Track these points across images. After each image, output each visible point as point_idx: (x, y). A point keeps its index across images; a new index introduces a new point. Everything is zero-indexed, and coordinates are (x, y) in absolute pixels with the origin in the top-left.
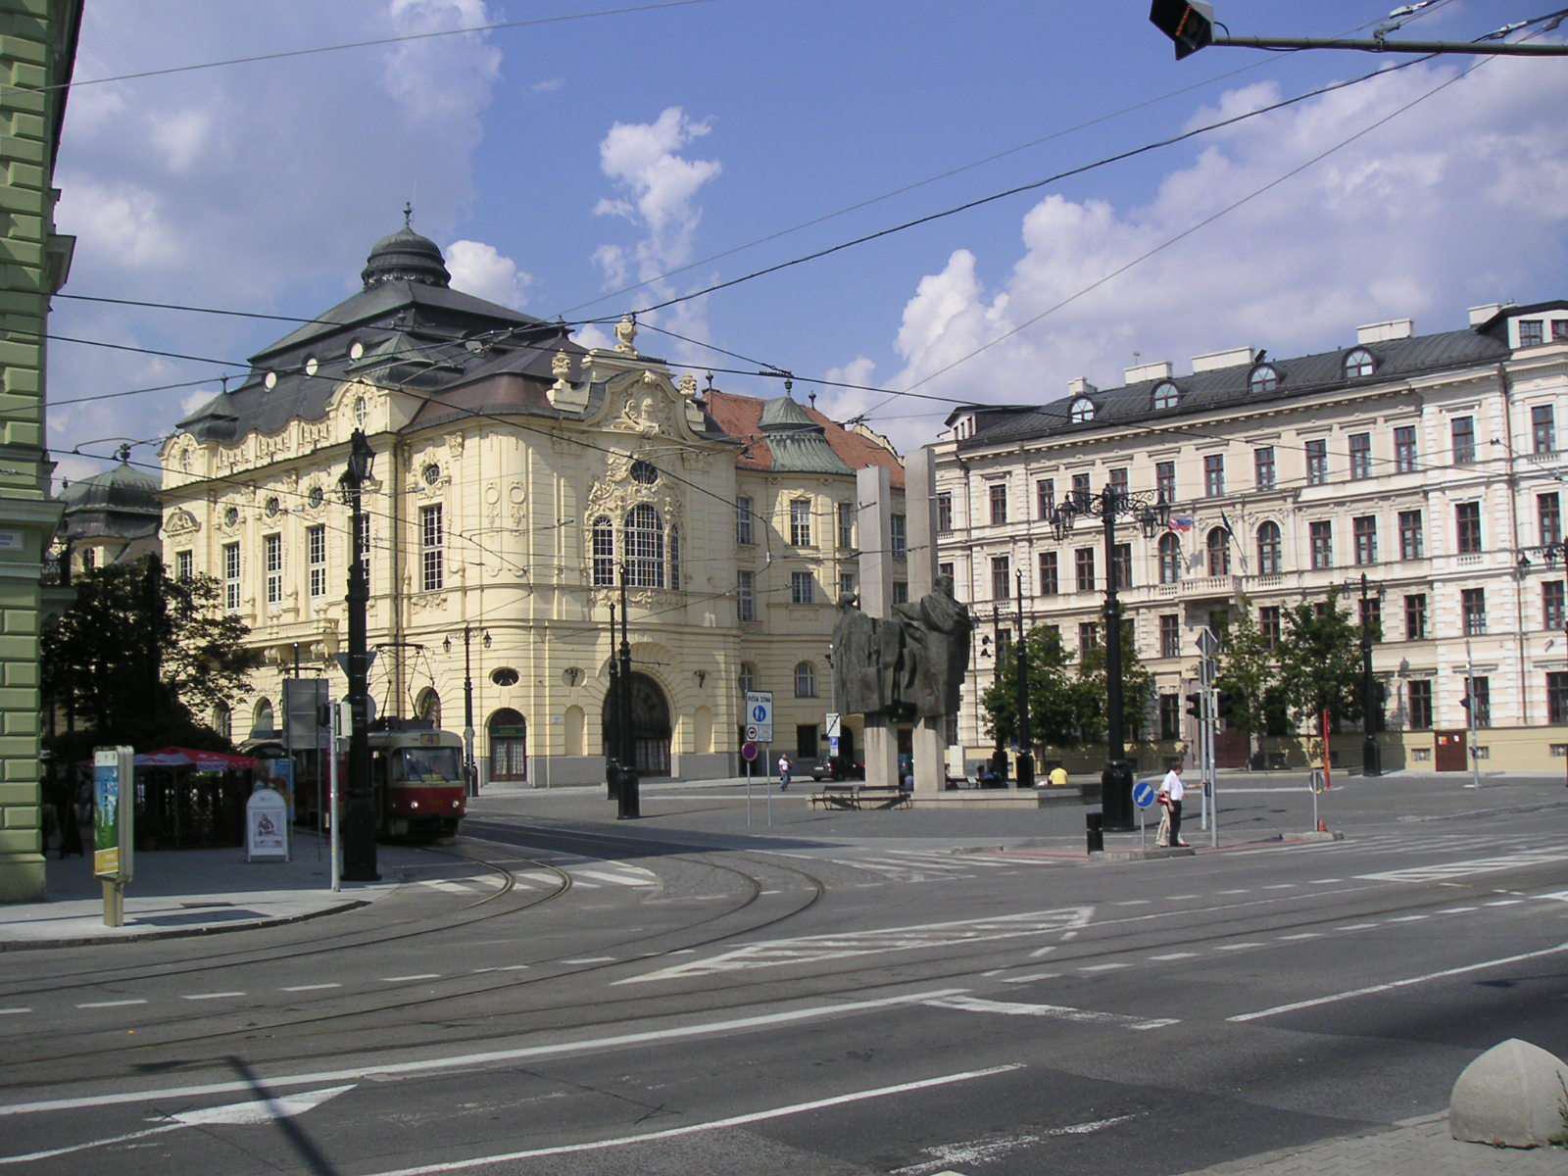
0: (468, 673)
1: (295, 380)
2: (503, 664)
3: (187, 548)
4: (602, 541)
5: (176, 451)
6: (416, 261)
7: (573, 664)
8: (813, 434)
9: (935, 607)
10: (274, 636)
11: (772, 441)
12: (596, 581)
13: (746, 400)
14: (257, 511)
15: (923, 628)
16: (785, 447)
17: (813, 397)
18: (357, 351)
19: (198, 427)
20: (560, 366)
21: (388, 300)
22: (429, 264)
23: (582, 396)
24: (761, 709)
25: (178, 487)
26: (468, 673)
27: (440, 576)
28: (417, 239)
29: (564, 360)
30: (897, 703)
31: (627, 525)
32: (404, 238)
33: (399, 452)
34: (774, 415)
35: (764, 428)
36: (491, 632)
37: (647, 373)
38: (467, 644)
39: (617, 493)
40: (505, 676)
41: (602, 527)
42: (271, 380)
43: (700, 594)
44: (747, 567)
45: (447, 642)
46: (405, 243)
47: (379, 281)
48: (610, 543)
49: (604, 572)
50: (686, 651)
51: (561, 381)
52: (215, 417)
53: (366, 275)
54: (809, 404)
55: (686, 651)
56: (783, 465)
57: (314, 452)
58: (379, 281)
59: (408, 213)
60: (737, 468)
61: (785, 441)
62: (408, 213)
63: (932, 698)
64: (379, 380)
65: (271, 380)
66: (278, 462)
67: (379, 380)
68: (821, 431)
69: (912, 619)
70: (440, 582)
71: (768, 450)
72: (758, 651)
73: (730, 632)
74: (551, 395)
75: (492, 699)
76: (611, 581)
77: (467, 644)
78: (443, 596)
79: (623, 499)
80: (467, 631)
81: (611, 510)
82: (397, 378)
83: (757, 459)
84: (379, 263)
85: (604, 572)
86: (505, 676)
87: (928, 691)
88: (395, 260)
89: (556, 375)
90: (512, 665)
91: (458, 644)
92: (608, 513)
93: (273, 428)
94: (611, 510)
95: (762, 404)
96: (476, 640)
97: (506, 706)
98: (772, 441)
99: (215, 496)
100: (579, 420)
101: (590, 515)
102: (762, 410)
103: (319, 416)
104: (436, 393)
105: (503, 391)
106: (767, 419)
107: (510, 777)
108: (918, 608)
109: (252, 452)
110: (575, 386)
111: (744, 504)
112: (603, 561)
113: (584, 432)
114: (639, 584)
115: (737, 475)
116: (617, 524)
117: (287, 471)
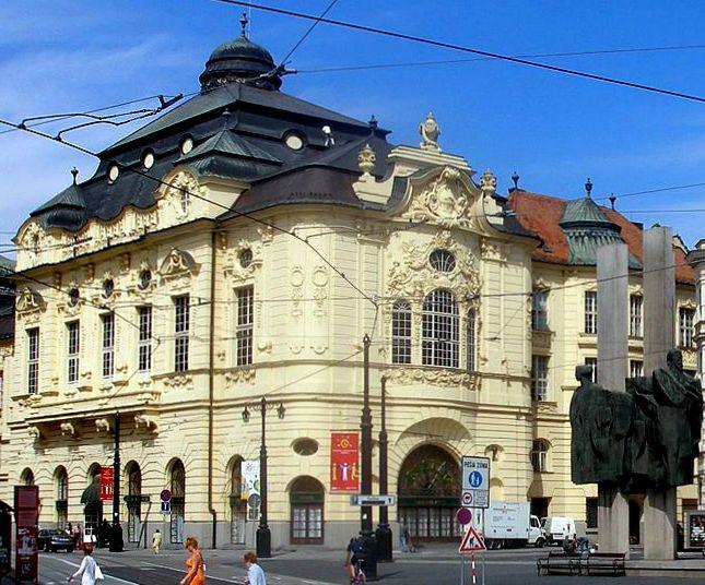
0: (263, 442)
1: (131, 176)
2: (304, 434)
3: (35, 325)
4: (401, 324)
5: (28, 237)
8: (610, 232)
9: (666, 381)
10: (105, 407)
11: (571, 237)
12: (395, 360)
13: (549, 200)
14: (95, 292)
15: (654, 401)
16: (583, 242)
17: (613, 200)
18: (188, 146)
19: (47, 215)
20: (367, 160)
21: (220, 100)
23: (387, 187)
24: (477, 475)
25: (28, 270)
26: (263, 442)
27: (250, 353)
28: (250, 46)
29: (369, 154)
30: (627, 473)
31: (425, 309)
32: (239, 45)
33: (217, 237)
34: (575, 213)
35: (565, 226)
36: (285, 406)
37: (447, 169)
38: (263, 415)
40: (305, 446)
42: (114, 173)
43: (492, 376)
44: (541, 351)
45: (246, 413)
46: (241, 50)
47: (215, 84)
48: (409, 325)
49: (402, 352)
50: (478, 427)
51: (366, 174)
52: (60, 206)
53: (203, 78)
54: (608, 205)
55: (478, 427)
56: (580, 260)
57: (142, 237)
58: (215, 84)
59: (244, 23)
60: (533, 260)
61: (583, 238)
62: (244, 23)
63: (660, 471)
64: (201, 171)
65: (114, 173)
66: (114, 246)
67: (201, 171)
68: (617, 229)
69: (646, 392)
70: (250, 358)
71: (566, 245)
72: (552, 430)
73: (522, 411)
74: (356, 186)
75: (288, 467)
76: (408, 360)
77: (263, 415)
78: (252, 371)
80: (264, 403)
82: (218, 169)
83: (556, 253)
85: (402, 352)
86: (305, 446)
87: (658, 463)
89: (362, 168)
90: (312, 436)
91: (255, 414)
93: (111, 219)
95: (564, 205)
96: (272, 412)
98: (571, 237)
99: (60, 278)
100: (381, 210)
102: (565, 210)
103: (149, 206)
104: (253, 184)
105: (318, 181)
106: (568, 218)
107: (308, 540)
108: (650, 381)
109: (96, 236)
110: (379, 178)
111: (538, 294)
113: (388, 221)
114: (435, 363)
115: (533, 267)
116: (416, 308)
117: (121, 255)
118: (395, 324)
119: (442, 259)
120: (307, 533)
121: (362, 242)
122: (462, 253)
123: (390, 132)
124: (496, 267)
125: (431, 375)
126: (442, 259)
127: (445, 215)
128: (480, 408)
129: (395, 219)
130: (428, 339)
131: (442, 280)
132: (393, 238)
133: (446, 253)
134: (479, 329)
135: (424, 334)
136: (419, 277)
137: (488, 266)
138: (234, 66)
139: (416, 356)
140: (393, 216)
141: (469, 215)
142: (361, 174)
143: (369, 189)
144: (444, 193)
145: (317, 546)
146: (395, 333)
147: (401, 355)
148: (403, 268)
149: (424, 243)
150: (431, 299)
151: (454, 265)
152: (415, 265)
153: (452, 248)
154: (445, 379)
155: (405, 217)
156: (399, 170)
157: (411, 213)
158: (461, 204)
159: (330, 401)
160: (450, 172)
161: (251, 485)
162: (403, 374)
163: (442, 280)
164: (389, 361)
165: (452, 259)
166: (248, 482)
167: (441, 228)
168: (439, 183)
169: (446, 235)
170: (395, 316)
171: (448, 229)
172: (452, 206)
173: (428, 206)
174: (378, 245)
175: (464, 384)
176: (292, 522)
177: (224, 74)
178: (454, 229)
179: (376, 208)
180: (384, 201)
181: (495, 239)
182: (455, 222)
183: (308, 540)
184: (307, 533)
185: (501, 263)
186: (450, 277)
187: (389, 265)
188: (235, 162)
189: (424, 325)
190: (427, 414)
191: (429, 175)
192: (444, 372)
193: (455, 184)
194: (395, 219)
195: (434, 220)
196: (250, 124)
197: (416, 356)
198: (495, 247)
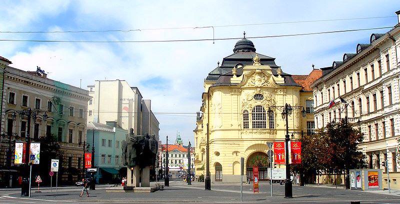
4: (246, 117)
6: (246, 46)
7: (218, 151)
22: (249, 47)
40: (218, 154)
48: (248, 117)
74: (232, 79)
84: (237, 47)
88: (242, 46)
92: (247, 109)
107: (219, 180)
116: (250, 112)
118: (244, 117)
119: (258, 96)
121: (232, 95)
125: (254, 131)
127: (258, 84)
131: (259, 103)
132: (242, 93)
134: (276, 117)
135: (253, 119)
136: (251, 102)
142: (233, 75)
143: (235, 80)
144: (257, 77)
147: (246, 126)
149: (252, 93)
155: (245, 86)
157: (247, 84)
160: (257, 71)
163: (259, 103)
164: (242, 128)
167: (257, 87)
169: (259, 89)
170: (244, 115)
177: (239, 49)
178: (261, 87)
179: (236, 85)
180: (240, 82)
183: (219, 180)
189: (253, 117)
191: (253, 72)
193: (260, 74)
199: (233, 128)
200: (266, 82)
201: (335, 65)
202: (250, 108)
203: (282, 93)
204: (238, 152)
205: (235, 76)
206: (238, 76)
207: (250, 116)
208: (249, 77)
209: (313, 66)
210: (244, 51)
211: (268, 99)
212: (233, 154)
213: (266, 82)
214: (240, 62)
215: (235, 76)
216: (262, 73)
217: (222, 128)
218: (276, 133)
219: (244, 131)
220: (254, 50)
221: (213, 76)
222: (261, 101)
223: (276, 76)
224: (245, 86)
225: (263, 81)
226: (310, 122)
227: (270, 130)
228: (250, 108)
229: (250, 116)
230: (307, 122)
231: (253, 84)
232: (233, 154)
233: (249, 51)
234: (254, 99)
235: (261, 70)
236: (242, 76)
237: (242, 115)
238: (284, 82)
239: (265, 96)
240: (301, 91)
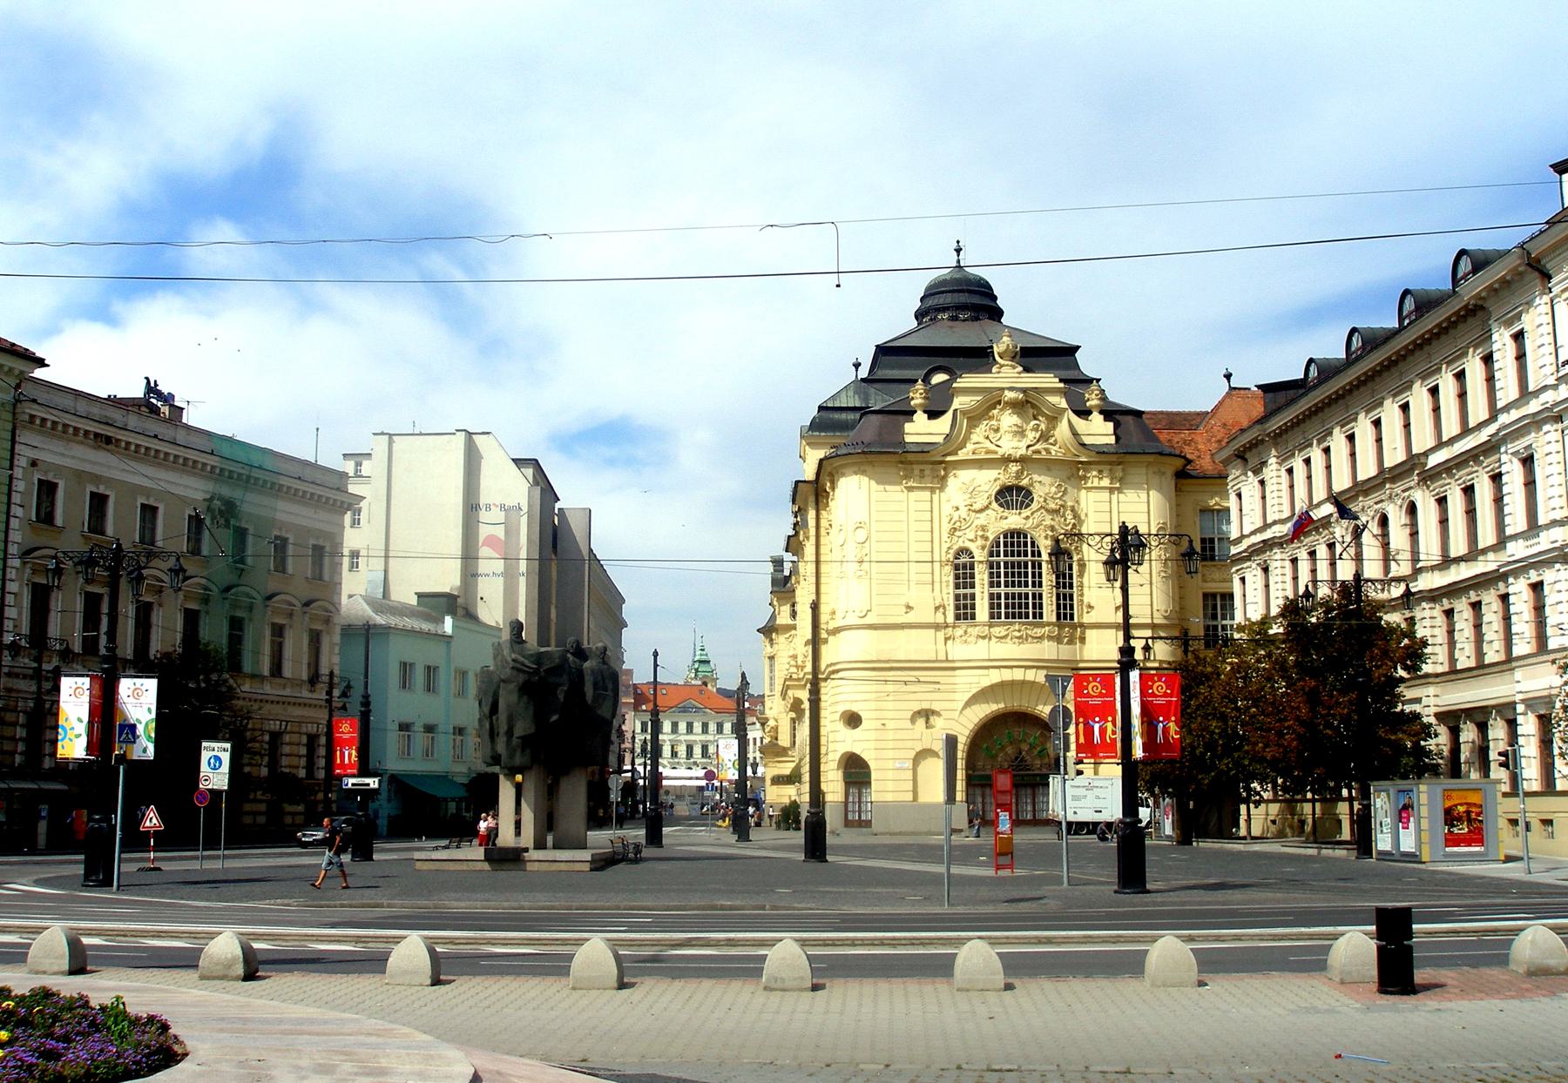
4: (963, 574)
6: (963, 298)
7: (855, 708)
12: (957, 617)
22: (976, 300)
37: (1006, 392)
39: (977, 522)
40: (853, 720)
41: (964, 559)
48: (972, 576)
49: (965, 607)
74: (908, 427)
79: (983, 528)
81: (971, 540)
84: (930, 302)
85: (965, 607)
92: (969, 545)
94: (971, 540)
97: (858, 752)
101: (949, 548)
112: (965, 596)
115: (1178, 490)
116: (980, 555)
118: (957, 577)
119: (1013, 496)
120: (860, 816)
121: (910, 489)
122: (1043, 486)
123: (1078, 347)
124: (1105, 495)
125: (998, 631)
126: (1013, 496)
127: (1011, 445)
128: (1081, 665)
129: (949, 458)
130: (995, 590)
131: (1014, 520)
132: (951, 481)
133: (1020, 489)
134: (1081, 575)
135: (991, 585)
136: (982, 519)
137: (1093, 495)
138: (936, 301)
139: (982, 611)
140: (945, 455)
141: (1051, 441)
142: (915, 412)
143: (920, 429)
144: (1008, 420)
145: (864, 830)
146: (957, 586)
147: (965, 611)
148: (963, 512)
149: (989, 480)
150: (998, 546)
151: (1032, 500)
152: (977, 507)
153: (1024, 482)
154: (1017, 634)
155: (962, 455)
156: (959, 402)
157: (970, 447)
158: (1036, 429)
159: (874, 669)
160: (1009, 395)
161: (730, 764)
162: (966, 632)
163: (1014, 520)
164: (951, 618)
165: (1029, 493)
166: (726, 761)
167: (1006, 460)
168: (1001, 410)
169: (1014, 468)
170: (957, 567)
171: (1016, 461)
172: (1021, 433)
173: (987, 438)
174: (932, 490)
175: (1050, 638)
176: (846, 803)
178: (1022, 460)
179: (924, 449)
181: (1099, 463)
182: (1023, 451)
184: (860, 816)
185: (1111, 490)
186: (1024, 515)
187: (947, 510)
188: (844, 416)
189: (991, 575)
190: (995, 677)
191: (992, 401)
192: (1017, 627)
193: (1017, 407)
194: (949, 458)
195: (996, 453)
196: (893, 368)
197: (982, 611)
198: (1100, 472)
199: (911, 618)
200: (1044, 437)
201: (1313, 372)
202: (980, 542)
203: (1106, 482)
204: (934, 712)
205: (920, 417)
206: (933, 414)
207: (981, 576)
208: (975, 417)
209: (1228, 376)
210: (954, 319)
211: (1052, 506)
212: (913, 720)
213: (1044, 437)
214: (940, 361)
215: (920, 417)
216: (1027, 404)
217: (869, 620)
218: (1083, 640)
219: (959, 632)
220: (997, 314)
221: (837, 416)
222: (1025, 512)
223: (1084, 413)
224: (962, 455)
225: (1031, 436)
226: (1214, 595)
227: (1061, 627)
228: (980, 542)
229: (981, 576)
230: (1205, 596)
231: (993, 447)
232: (913, 720)
233: (977, 319)
234: (995, 505)
235: (1024, 391)
236: (948, 416)
237: (948, 569)
238: (1112, 440)
239: (1038, 492)
240: (1182, 475)
